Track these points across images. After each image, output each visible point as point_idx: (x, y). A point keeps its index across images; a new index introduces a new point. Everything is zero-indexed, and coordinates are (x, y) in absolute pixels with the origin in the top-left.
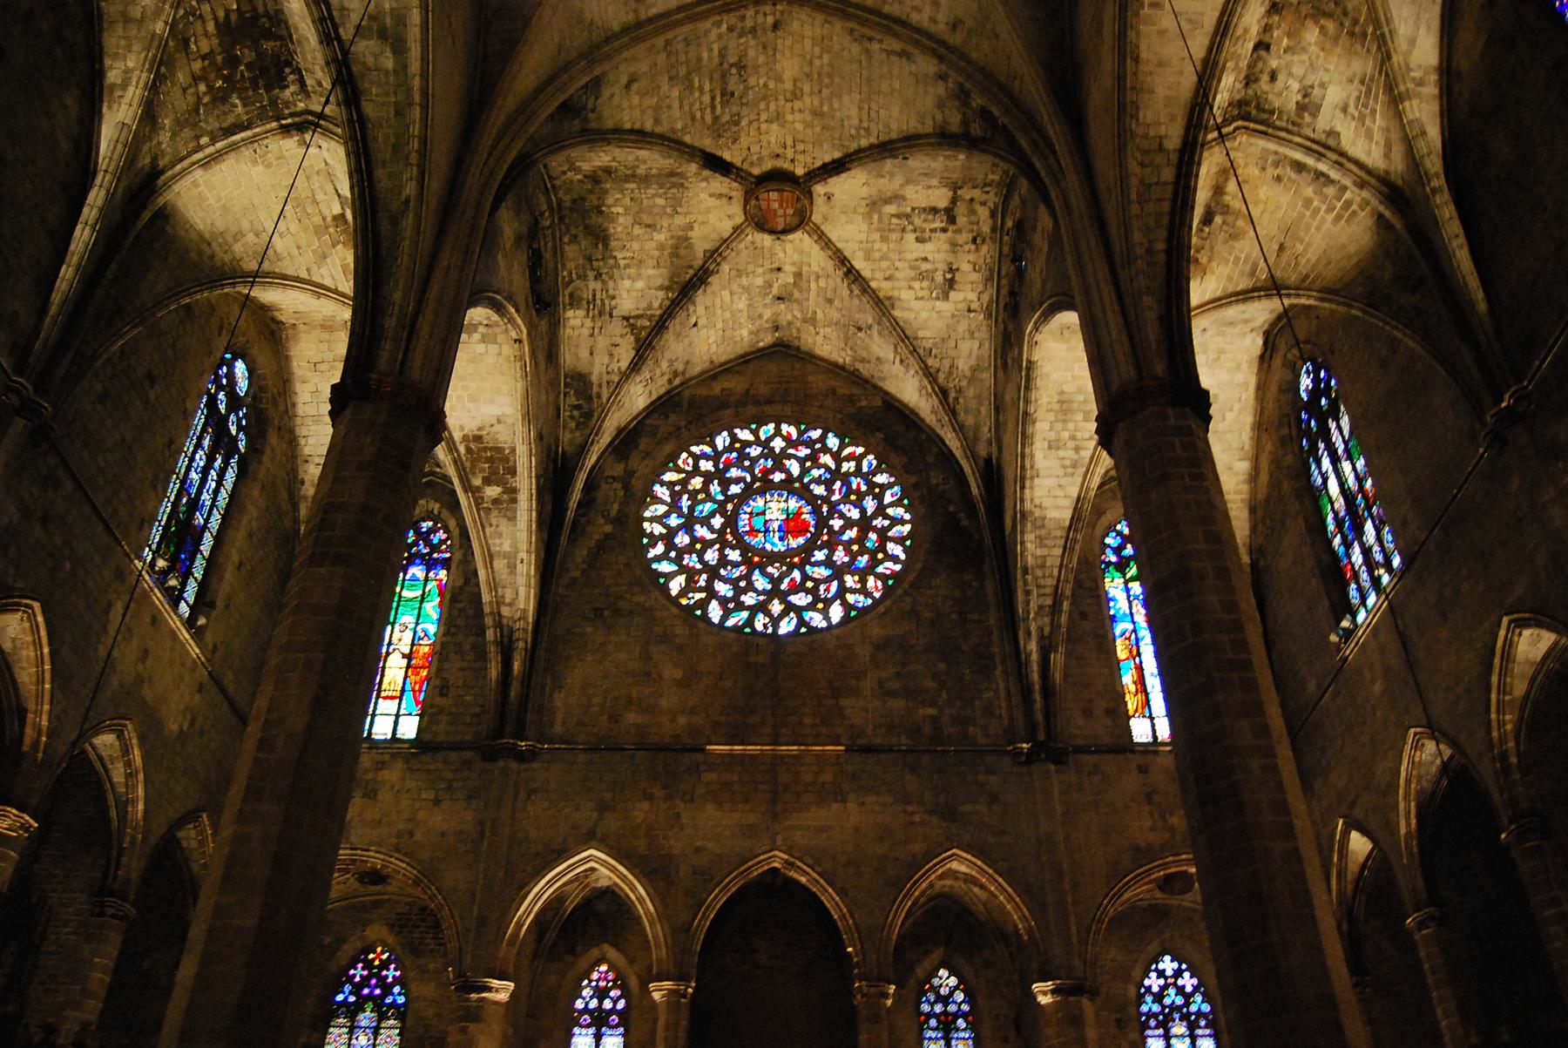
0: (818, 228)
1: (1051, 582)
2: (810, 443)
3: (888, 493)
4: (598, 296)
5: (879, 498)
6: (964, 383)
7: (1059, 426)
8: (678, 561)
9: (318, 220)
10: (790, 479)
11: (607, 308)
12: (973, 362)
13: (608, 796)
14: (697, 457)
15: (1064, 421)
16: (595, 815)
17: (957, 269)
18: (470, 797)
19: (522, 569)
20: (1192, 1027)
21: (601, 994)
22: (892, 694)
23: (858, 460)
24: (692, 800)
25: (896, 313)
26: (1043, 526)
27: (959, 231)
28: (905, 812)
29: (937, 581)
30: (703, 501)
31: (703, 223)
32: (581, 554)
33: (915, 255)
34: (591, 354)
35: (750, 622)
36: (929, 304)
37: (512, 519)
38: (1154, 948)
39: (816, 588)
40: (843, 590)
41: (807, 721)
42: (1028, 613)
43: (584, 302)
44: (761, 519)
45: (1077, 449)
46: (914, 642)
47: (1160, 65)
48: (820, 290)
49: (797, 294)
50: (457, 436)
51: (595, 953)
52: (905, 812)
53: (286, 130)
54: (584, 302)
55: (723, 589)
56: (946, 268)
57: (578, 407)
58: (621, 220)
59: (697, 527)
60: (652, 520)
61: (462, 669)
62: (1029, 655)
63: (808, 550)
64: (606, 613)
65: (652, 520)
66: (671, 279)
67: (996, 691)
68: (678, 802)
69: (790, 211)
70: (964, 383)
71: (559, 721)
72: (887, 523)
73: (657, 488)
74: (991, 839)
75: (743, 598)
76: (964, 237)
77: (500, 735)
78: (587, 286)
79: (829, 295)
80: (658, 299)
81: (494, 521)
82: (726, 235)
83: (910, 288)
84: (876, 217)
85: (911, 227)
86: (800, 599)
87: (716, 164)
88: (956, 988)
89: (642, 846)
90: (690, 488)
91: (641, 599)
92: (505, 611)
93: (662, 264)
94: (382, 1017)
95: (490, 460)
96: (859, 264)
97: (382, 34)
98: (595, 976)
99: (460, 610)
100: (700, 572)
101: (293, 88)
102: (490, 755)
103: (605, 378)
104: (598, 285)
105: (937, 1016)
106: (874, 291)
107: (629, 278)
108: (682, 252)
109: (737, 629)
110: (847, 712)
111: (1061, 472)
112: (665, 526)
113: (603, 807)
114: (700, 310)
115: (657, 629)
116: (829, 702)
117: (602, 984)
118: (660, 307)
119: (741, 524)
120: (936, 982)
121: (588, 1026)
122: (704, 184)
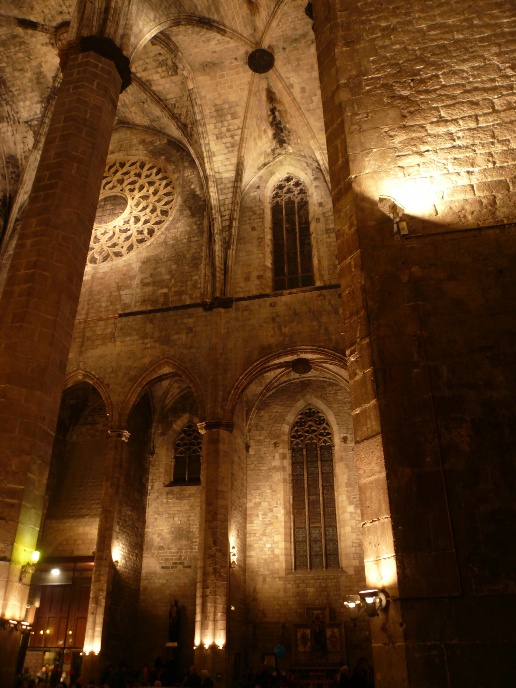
1: (228, 212)
4: (11, 114)
7: (219, 125)
15: (222, 122)
25: (154, 88)
26: (222, 183)
29: (178, 225)
33: (154, 53)
34: (15, 144)
36: (169, 80)
43: (5, 118)
45: (232, 136)
52: (143, 343)
54: (5, 118)
57: (13, 173)
58: (7, 70)
66: (41, 96)
67: (200, 275)
74: (185, 351)
78: (3, 109)
83: (157, 72)
87: (31, 25)
93: (34, 89)
103: (23, 155)
106: (139, 79)
107: (22, 100)
108: (42, 80)
110: (123, 297)
111: (226, 151)
118: (41, 113)
122: (34, 39)
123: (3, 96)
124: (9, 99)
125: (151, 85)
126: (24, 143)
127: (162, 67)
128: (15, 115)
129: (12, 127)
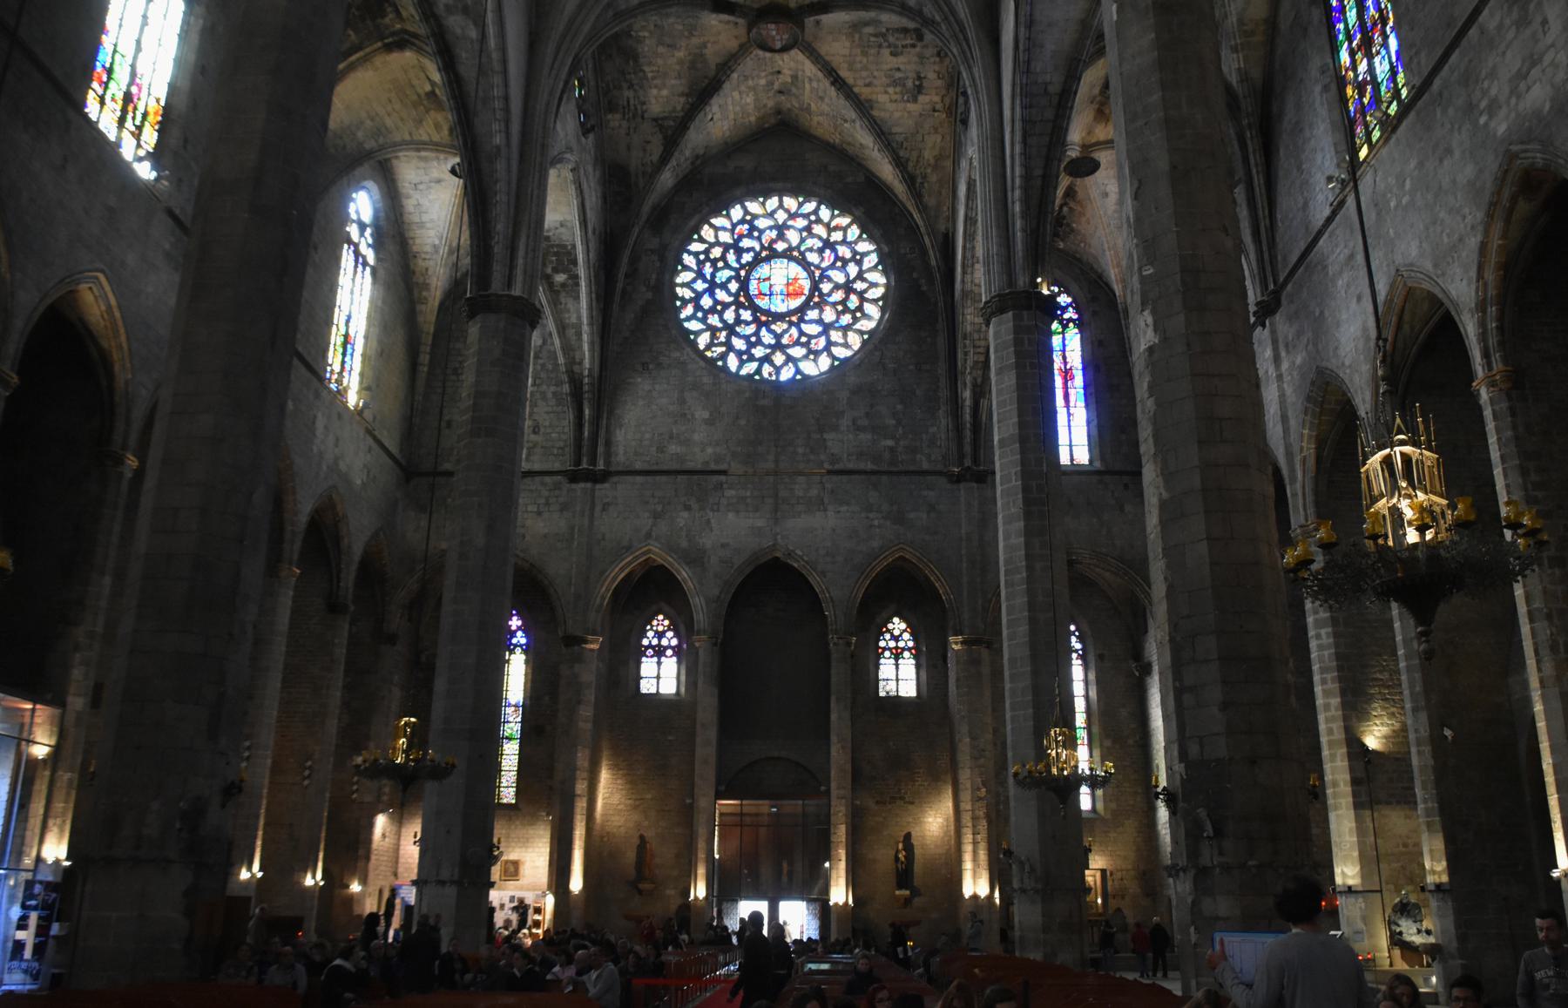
0: (810, 45)
2: (806, 216)
3: (866, 260)
4: (632, 102)
5: (859, 263)
6: (929, 171)
8: (704, 320)
9: (415, 97)
10: (790, 249)
11: (640, 112)
12: (936, 152)
13: (659, 508)
14: (717, 230)
16: (650, 521)
17: (925, 78)
18: (561, 511)
19: (585, 337)
21: (660, 635)
22: (859, 429)
23: (845, 229)
24: (718, 510)
25: (875, 113)
27: (926, 46)
28: (867, 518)
30: (722, 268)
31: (714, 42)
33: (889, 67)
35: (758, 371)
36: (901, 105)
37: (577, 298)
39: (808, 343)
40: (830, 344)
41: (800, 450)
42: (966, 368)
44: (767, 284)
46: (880, 388)
48: (812, 89)
49: (794, 90)
53: (389, 48)
55: (739, 344)
56: (915, 76)
58: (647, 42)
59: (718, 291)
60: (683, 285)
61: (547, 413)
62: (964, 401)
63: (801, 310)
64: (651, 366)
65: (683, 285)
68: (708, 511)
69: (786, 37)
70: (929, 171)
71: (621, 450)
72: (864, 286)
73: (685, 256)
75: (753, 351)
76: (929, 52)
79: (820, 94)
80: (680, 103)
81: (563, 300)
82: (734, 51)
83: (886, 92)
84: (857, 36)
85: (886, 44)
86: (797, 352)
88: (905, 631)
89: (684, 544)
90: (712, 257)
91: (678, 354)
92: (576, 368)
95: (556, 254)
96: (844, 73)
98: (655, 623)
99: (543, 366)
100: (720, 330)
101: (391, 16)
105: (890, 649)
106: (856, 96)
107: (656, 87)
108: (699, 66)
109: (750, 377)
110: (829, 444)
112: (694, 290)
113: (656, 516)
114: (715, 108)
115: (689, 379)
116: (816, 436)
117: (660, 628)
118: (683, 110)
119: (751, 288)
120: (890, 626)
121: (652, 656)
123: (628, 77)
124: (635, 82)
125: (872, 108)
126: (645, 150)
127: (895, 86)
128: (639, 107)
129: (628, 120)
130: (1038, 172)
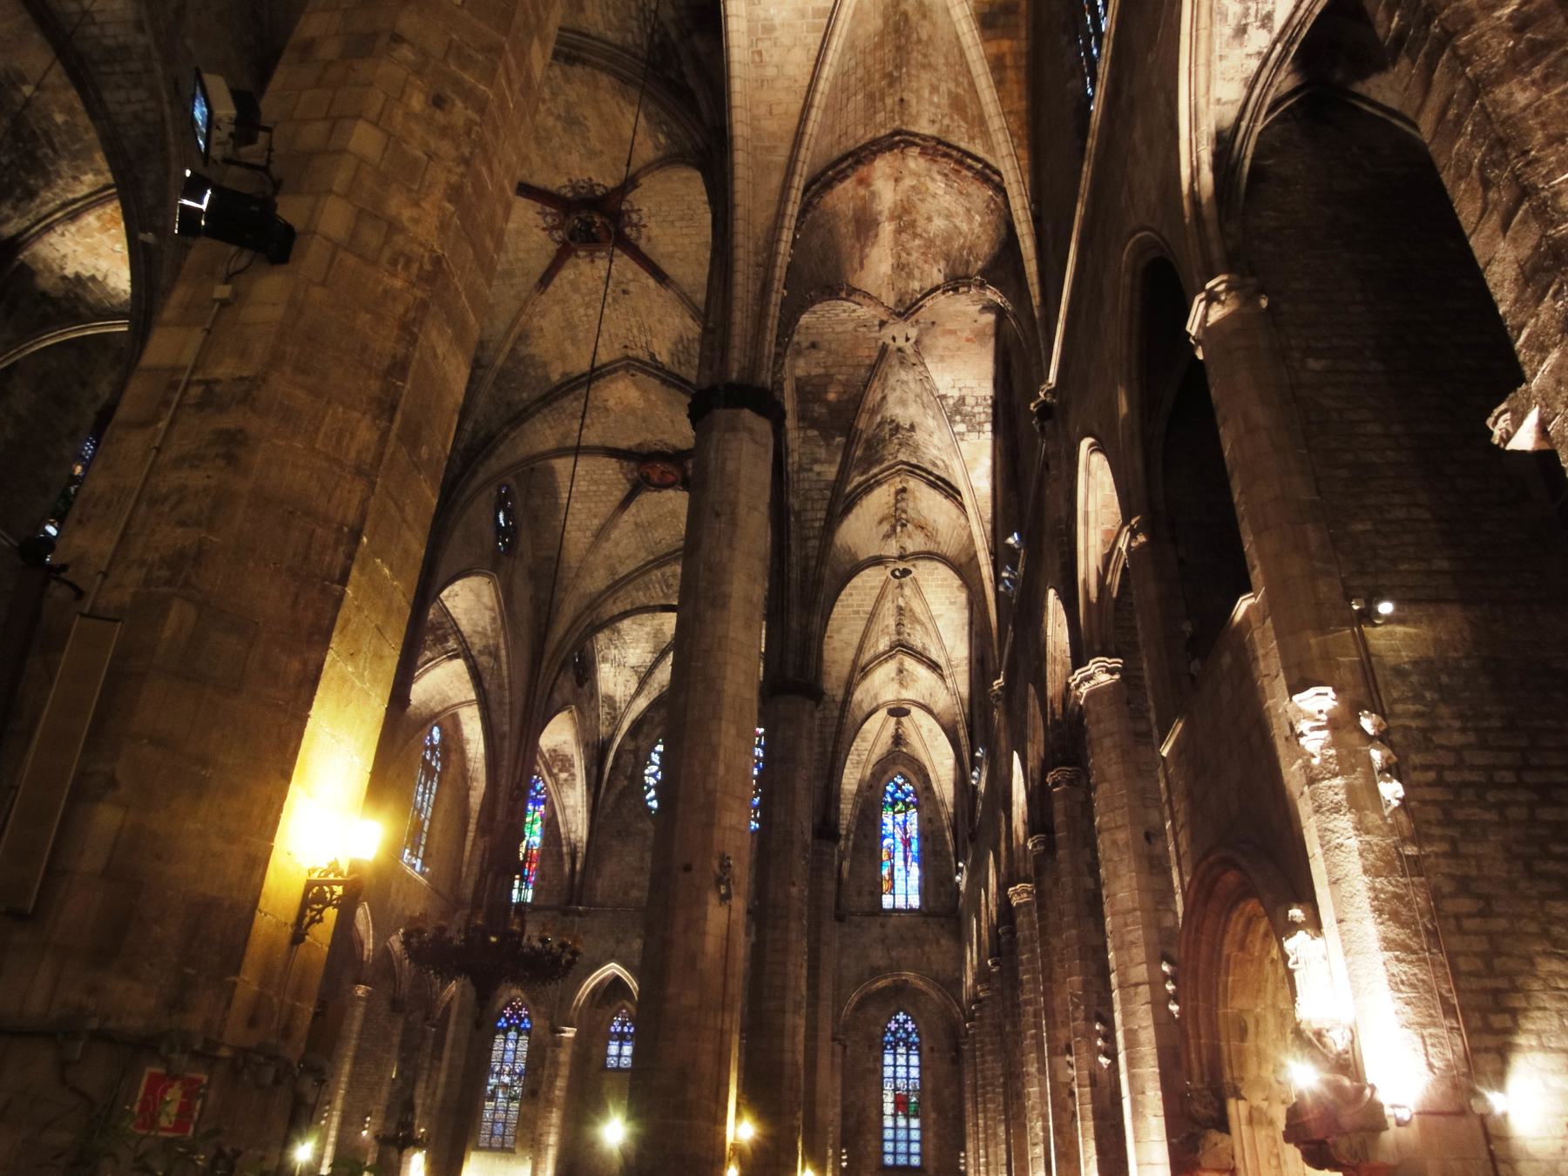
20: (909, 1049)
32: (611, 799)
38: (893, 1008)
47: (834, 662)
50: (544, 749)
51: (619, 1004)
60: (650, 775)
65: (650, 775)
77: (570, 902)
80: (648, 659)
91: (640, 825)
94: (519, 1034)
95: (561, 760)
97: (490, 654)
102: (565, 913)
104: (616, 652)
113: (618, 942)
130: (830, 749)
